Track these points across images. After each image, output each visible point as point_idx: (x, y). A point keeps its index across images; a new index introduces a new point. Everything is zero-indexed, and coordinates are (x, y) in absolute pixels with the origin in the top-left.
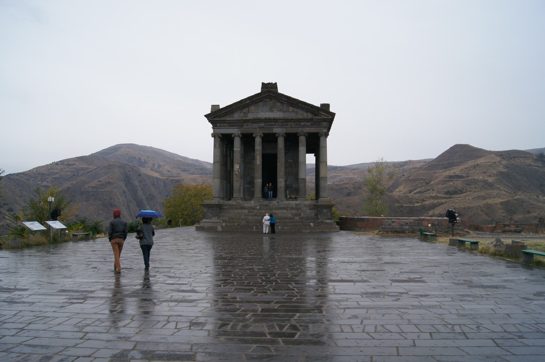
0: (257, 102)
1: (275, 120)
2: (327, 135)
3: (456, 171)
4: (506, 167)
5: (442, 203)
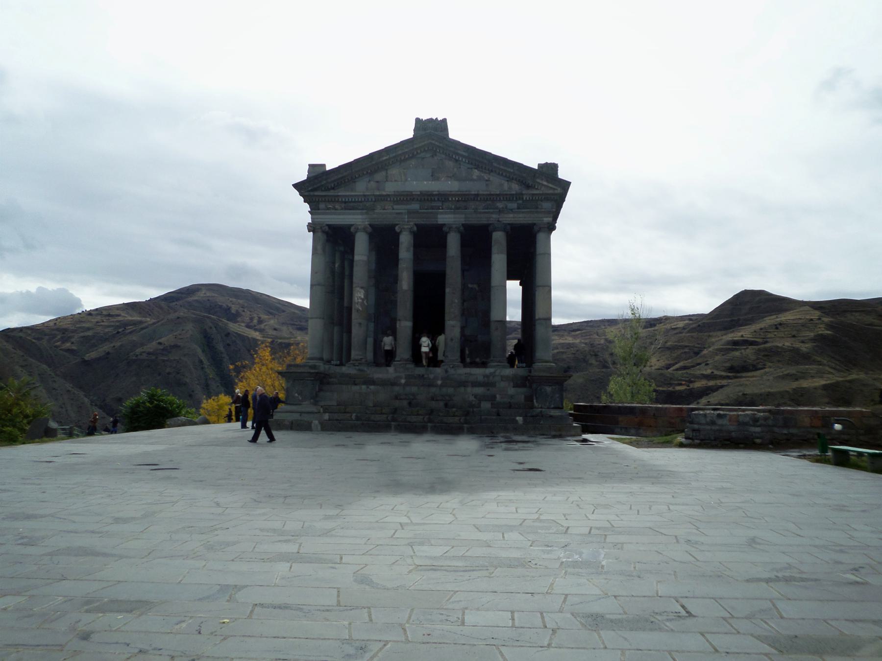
0: (405, 160)
1: (443, 197)
2: (552, 227)
3: (745, 332)
4: (829, 326)
5: (722, 387)
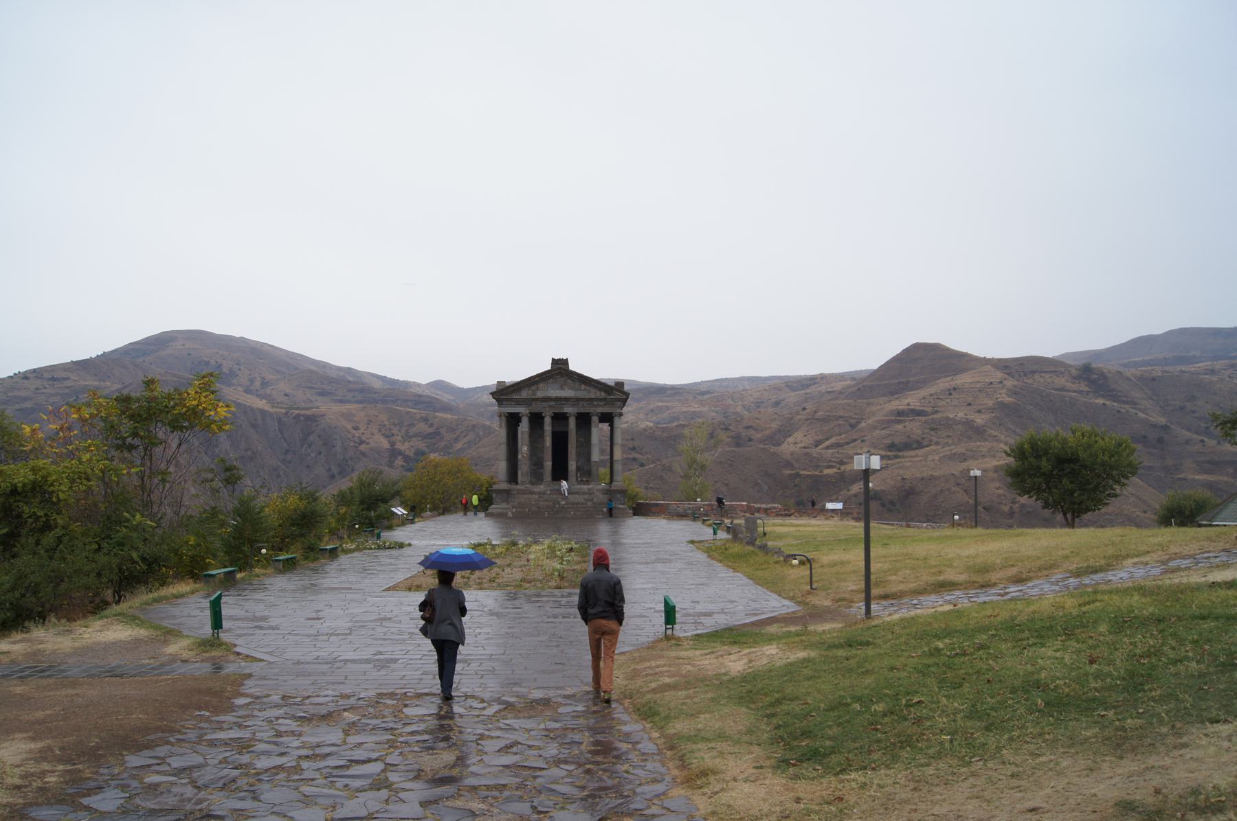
1: (567, 399)
3: (912, 400)
4: (1013, 392)
